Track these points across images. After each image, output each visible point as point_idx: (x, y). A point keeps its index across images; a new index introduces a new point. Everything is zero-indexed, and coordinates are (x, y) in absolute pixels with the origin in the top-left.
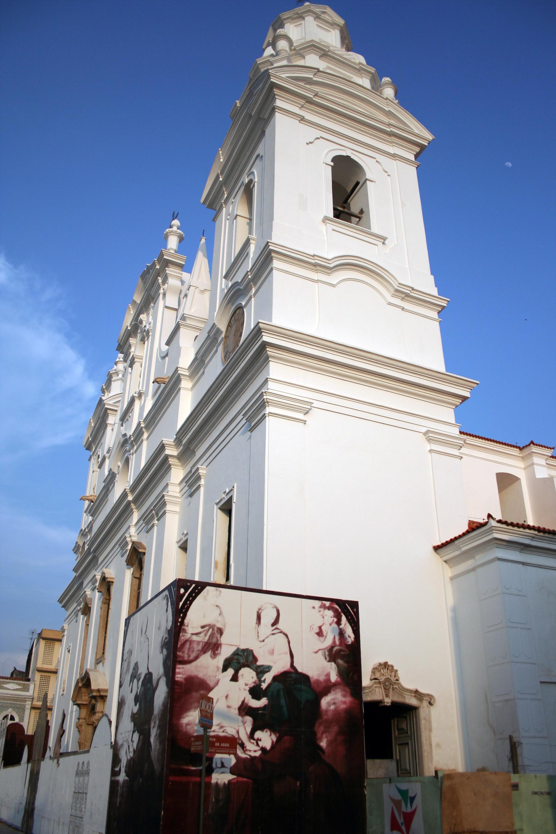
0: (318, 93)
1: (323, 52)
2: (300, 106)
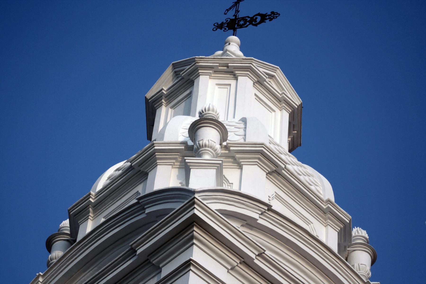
0: (264, 253)
1: (275, 169)
2: (229, 268)
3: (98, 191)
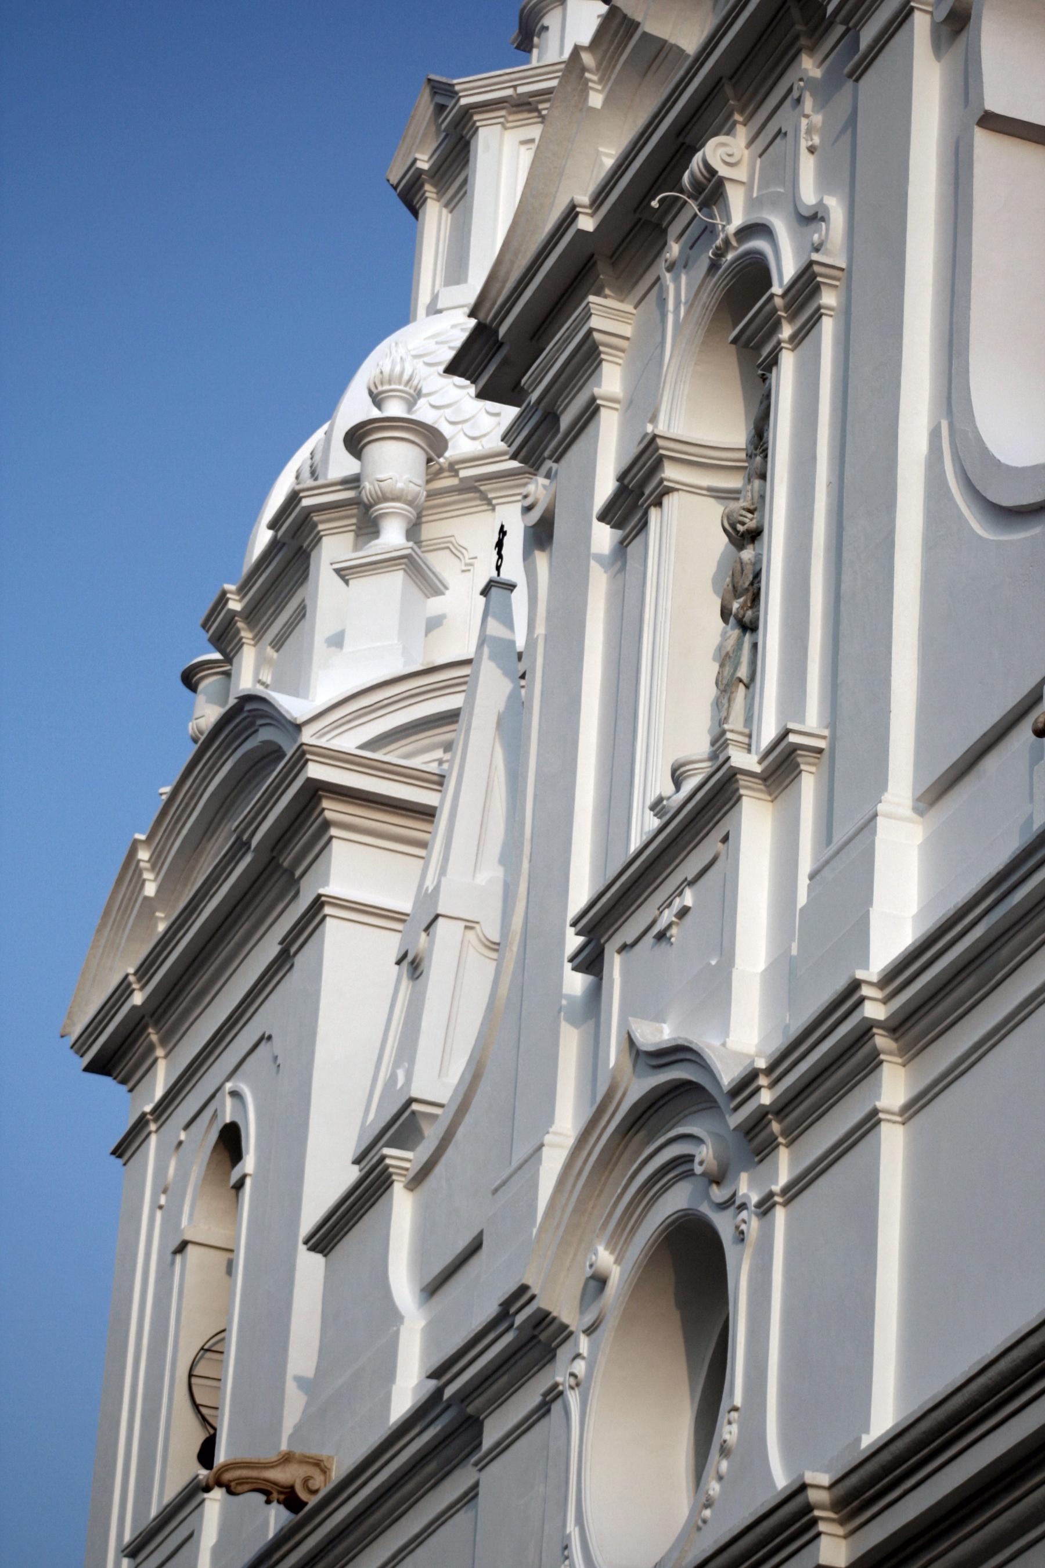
3: (257, 559)
